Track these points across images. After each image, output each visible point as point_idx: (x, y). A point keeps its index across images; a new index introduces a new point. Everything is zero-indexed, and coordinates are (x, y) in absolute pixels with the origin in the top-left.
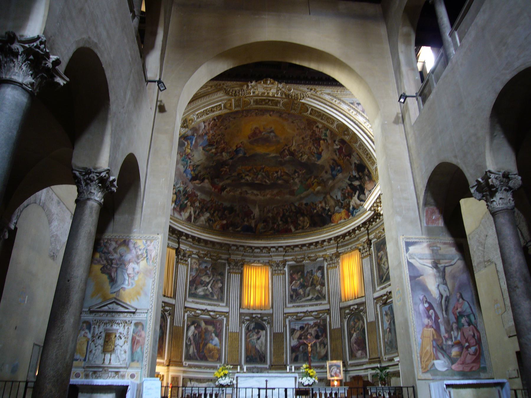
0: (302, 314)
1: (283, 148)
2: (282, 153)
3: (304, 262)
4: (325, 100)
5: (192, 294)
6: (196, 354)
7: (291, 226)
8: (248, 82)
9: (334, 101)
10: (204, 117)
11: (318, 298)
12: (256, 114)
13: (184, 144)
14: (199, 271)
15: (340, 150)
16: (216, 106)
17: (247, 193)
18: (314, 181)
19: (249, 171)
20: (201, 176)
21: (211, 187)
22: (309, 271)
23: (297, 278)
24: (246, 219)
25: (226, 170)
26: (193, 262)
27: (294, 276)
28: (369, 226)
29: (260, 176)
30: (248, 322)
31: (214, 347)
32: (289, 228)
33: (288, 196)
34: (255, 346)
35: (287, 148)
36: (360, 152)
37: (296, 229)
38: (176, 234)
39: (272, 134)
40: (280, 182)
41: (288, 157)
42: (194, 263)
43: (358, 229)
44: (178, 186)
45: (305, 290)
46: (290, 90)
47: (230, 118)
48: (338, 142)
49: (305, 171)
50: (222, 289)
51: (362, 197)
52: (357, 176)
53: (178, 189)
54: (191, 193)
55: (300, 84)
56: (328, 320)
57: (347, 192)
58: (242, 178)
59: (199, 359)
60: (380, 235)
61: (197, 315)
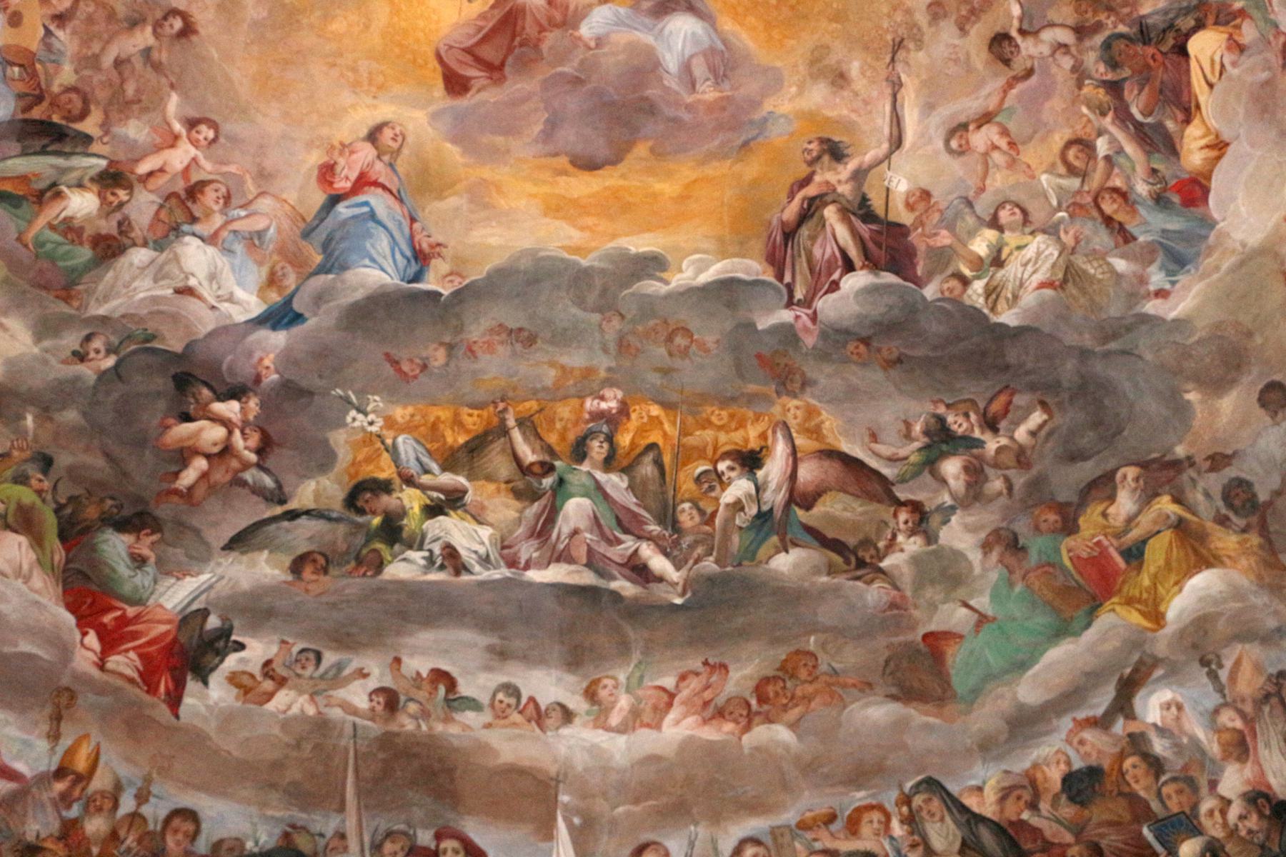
1: (806, 181)
17: (456, 702)
18: (1146, 522)
21: (70, 619)
25: (227, 450)
29: (576, 510)
35: (837, 177)
49: (1037, 418)
58: (392, 531)
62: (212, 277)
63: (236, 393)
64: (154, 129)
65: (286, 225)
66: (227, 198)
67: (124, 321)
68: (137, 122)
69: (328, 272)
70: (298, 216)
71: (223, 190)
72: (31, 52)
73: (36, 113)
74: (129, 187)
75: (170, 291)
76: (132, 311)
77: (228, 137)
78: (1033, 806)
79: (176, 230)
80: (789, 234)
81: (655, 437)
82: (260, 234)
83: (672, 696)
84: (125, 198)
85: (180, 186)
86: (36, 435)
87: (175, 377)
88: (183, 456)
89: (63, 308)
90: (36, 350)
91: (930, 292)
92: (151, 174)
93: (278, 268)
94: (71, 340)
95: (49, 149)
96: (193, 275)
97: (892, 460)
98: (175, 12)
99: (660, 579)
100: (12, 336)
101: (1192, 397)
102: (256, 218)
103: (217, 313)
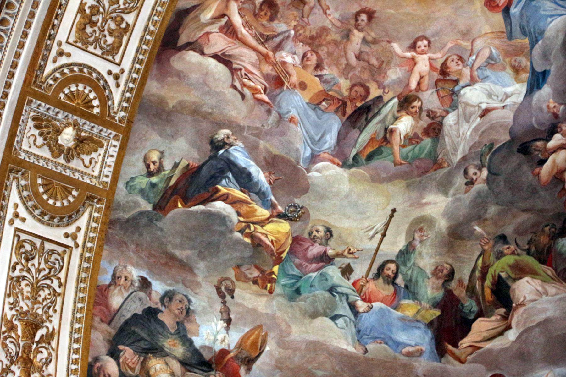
13: (222, 219)
20: (471, 291)
64: (400, 66)
65: (497, 42)
66: (461, 58)
67: (473, 151)
68: (391, 70)
69: (537, 41)
70: (498, 34)
71: (455, 57)
72: (321, 91)
73: (349, 111)
74: (417, 98)
75: (479, 119)
76: (471, 144)
77: (433, 36)
79: (453, 93)
82: (491, 57)
84: (420, 103)
85: (436, 75)
86: (486, 232)
87: (519, 151)
89: (442, 172)
90: (450, 199)
92: (419, 84)
93: (513, 63)
94: (460, 180)
95: (369, 118)
96: (481, 103)
98: (358, 14)
100: (435, 204)
102: (482, 53)
103: (508, 107)
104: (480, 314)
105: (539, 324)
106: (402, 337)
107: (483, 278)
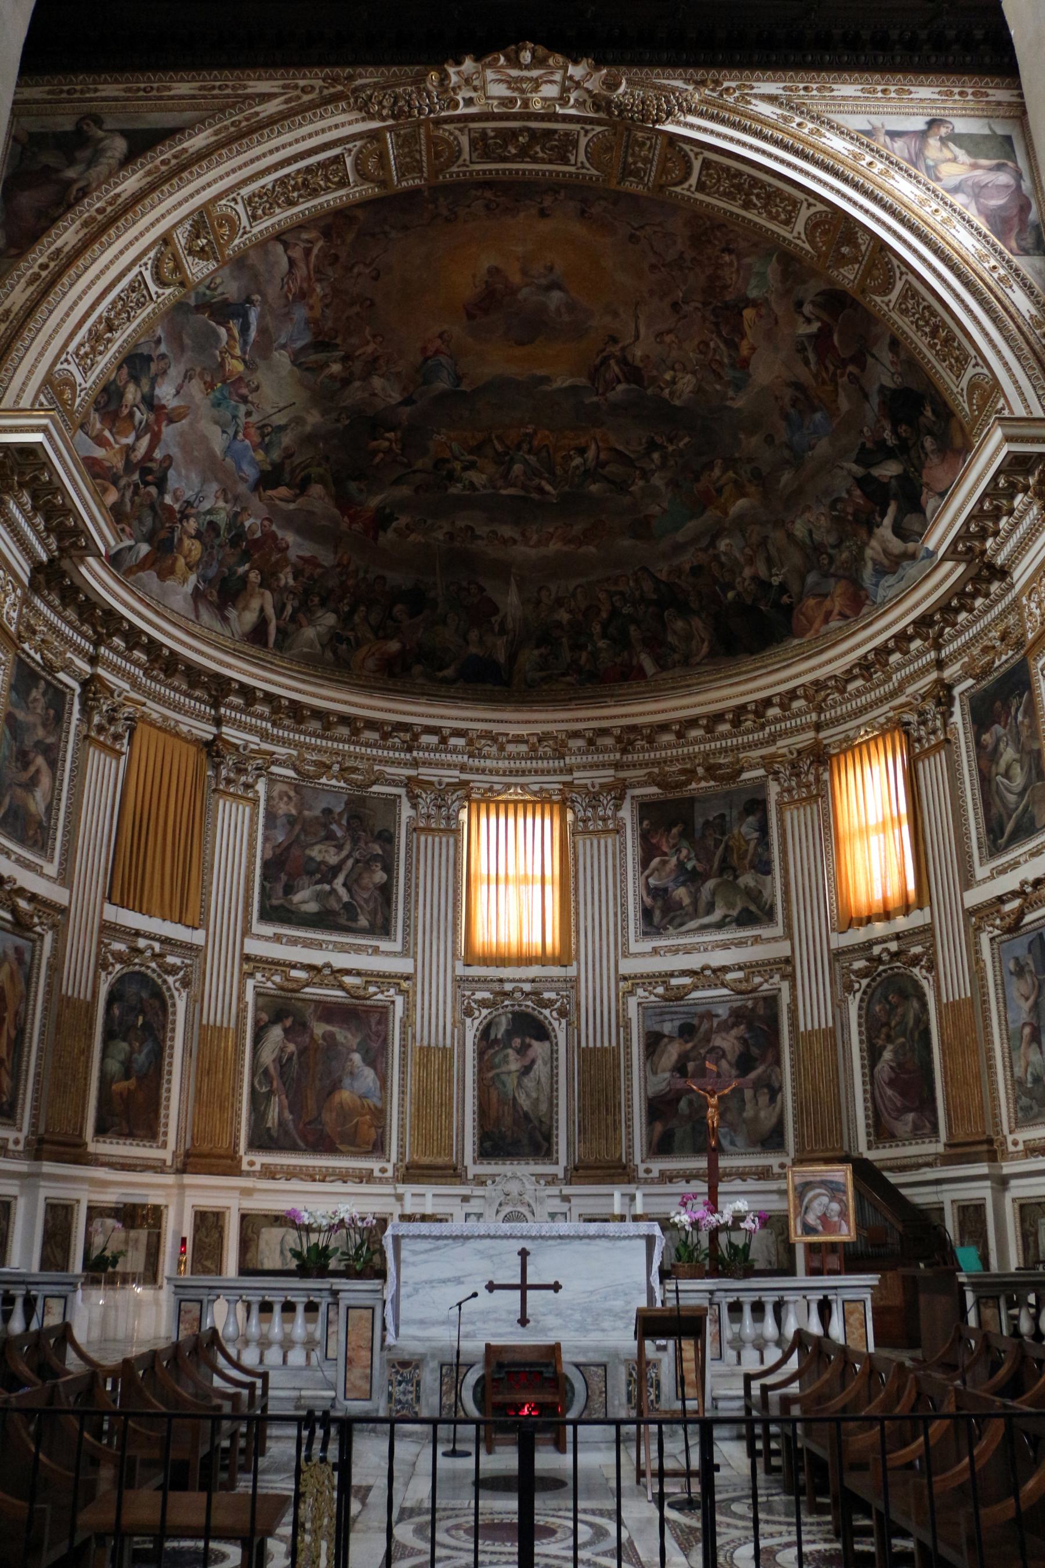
0: (687, 981)
2: (595, 373)
3: (694, 785)
4: (761, 122)
5: (275, 908)
6: (291, 1125)
7: (643, 656)
8: (445, 61)
9: (794, 125)
10: (282, 216)
11: (746, 919)
12: (487, 207)
14: (297, 828)
15: (821, 341)
16: (321, 165)
17: (475, 537)
19: (478, 450)
20: (293, 471)
21: (337, 512)
22: (711, 819)
23: (665, 849)
24: (474, 635)
26: (275, 794)
27: (654, 841)
28: (943, 628)
29: (517, 468)
30: (485, 1012)
31: (358, 1102)
32: (635, 662)
33: (626, 543)
34: (514, 1098)
35: (615, 349)
36: (904, 324)
37: (663, 668)
38: (208, 690)
39: (556, 295)
40: (594, 488)
41: (621, 387)
42: (281, 799)
43: (898, 649)
44: (206, 505)
45: (698, 890)
46: (614, 86)
47: (387, 228)
48: (813, 302)
49: (687, 440)
50: (386, 891)
51: (911, 521)
52: (891, 441)
53: (208, 518)
54: (259, 534)
55: (652, 64)
56: (785, 998)
57: (850, 510)
58: (451, 477)
59: (301, 1144)
60: (988, 664)
61: (294, 986)
62: (383, 389)
63: (392, 429)
73: (320, 338)
78: (679, 577)
80: (597, 369)
81: (547, 442)
83: (552, 535)
88: (375, 452)
91: (649, 392)
94: (334, 415)
97: (634, 452)
99: (548, 493)
101: (742, 436)
104: (286, 485)
105: (308, 511)
106: (245, 467)
107: (303, 470)
